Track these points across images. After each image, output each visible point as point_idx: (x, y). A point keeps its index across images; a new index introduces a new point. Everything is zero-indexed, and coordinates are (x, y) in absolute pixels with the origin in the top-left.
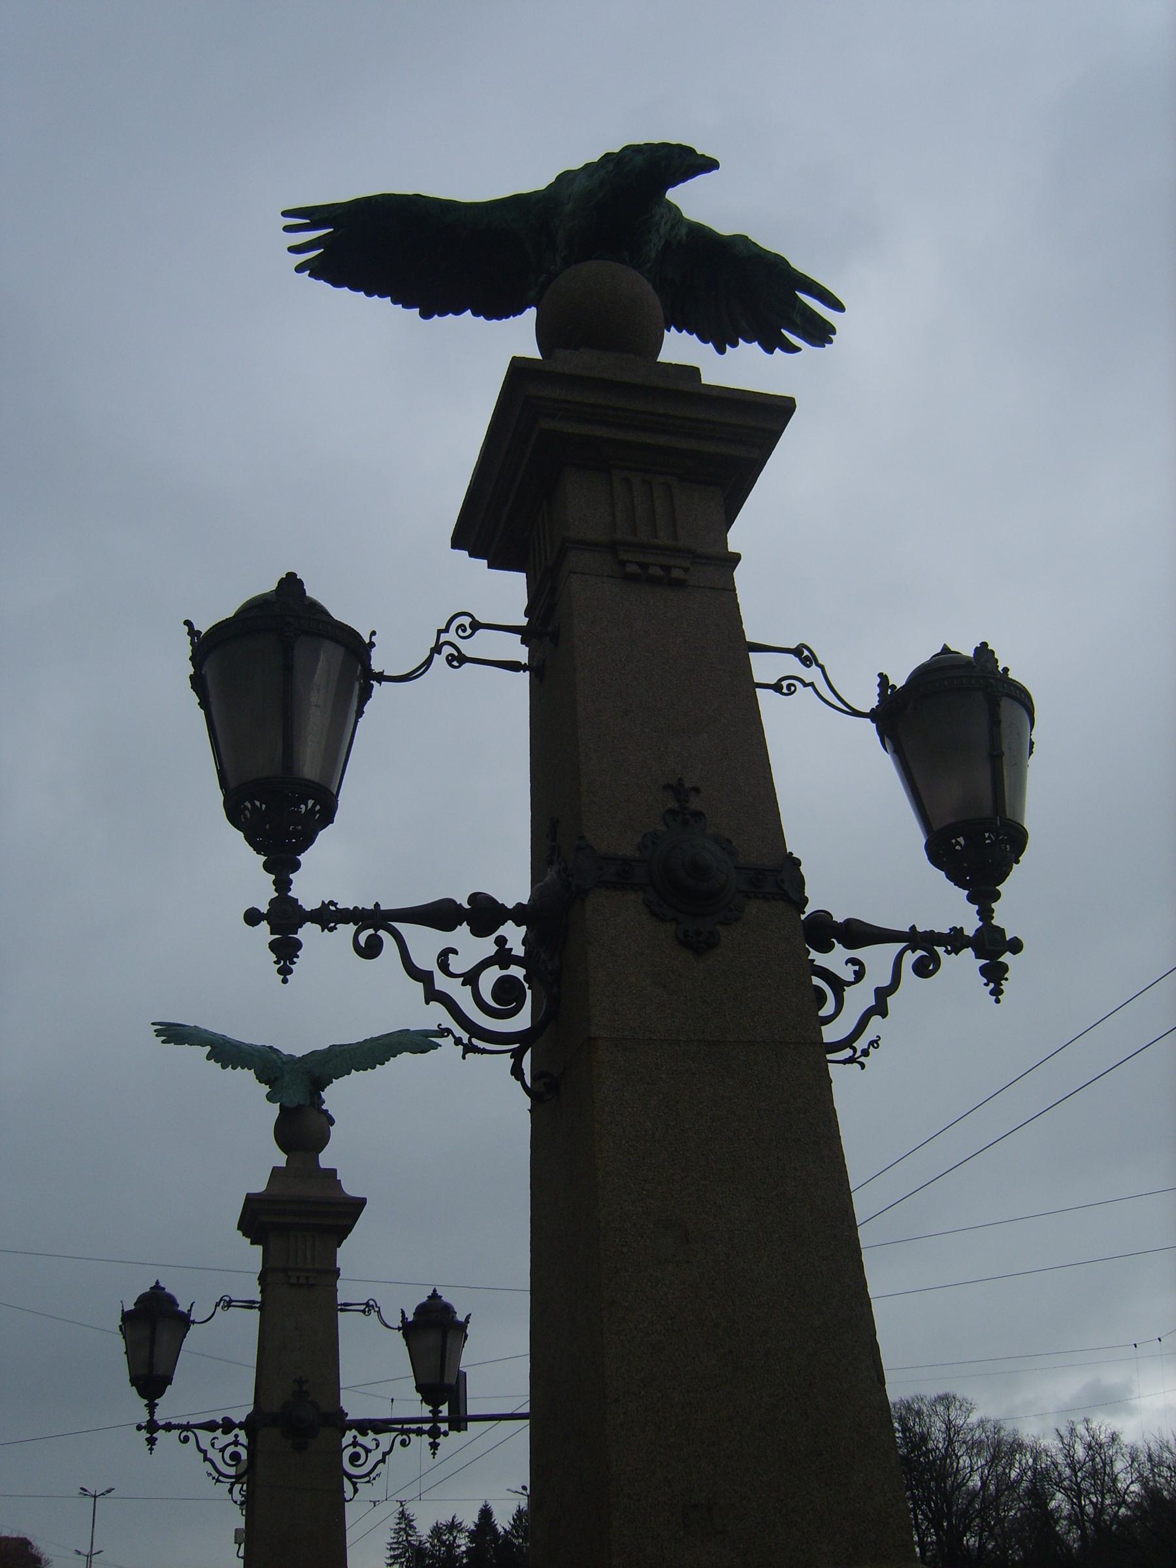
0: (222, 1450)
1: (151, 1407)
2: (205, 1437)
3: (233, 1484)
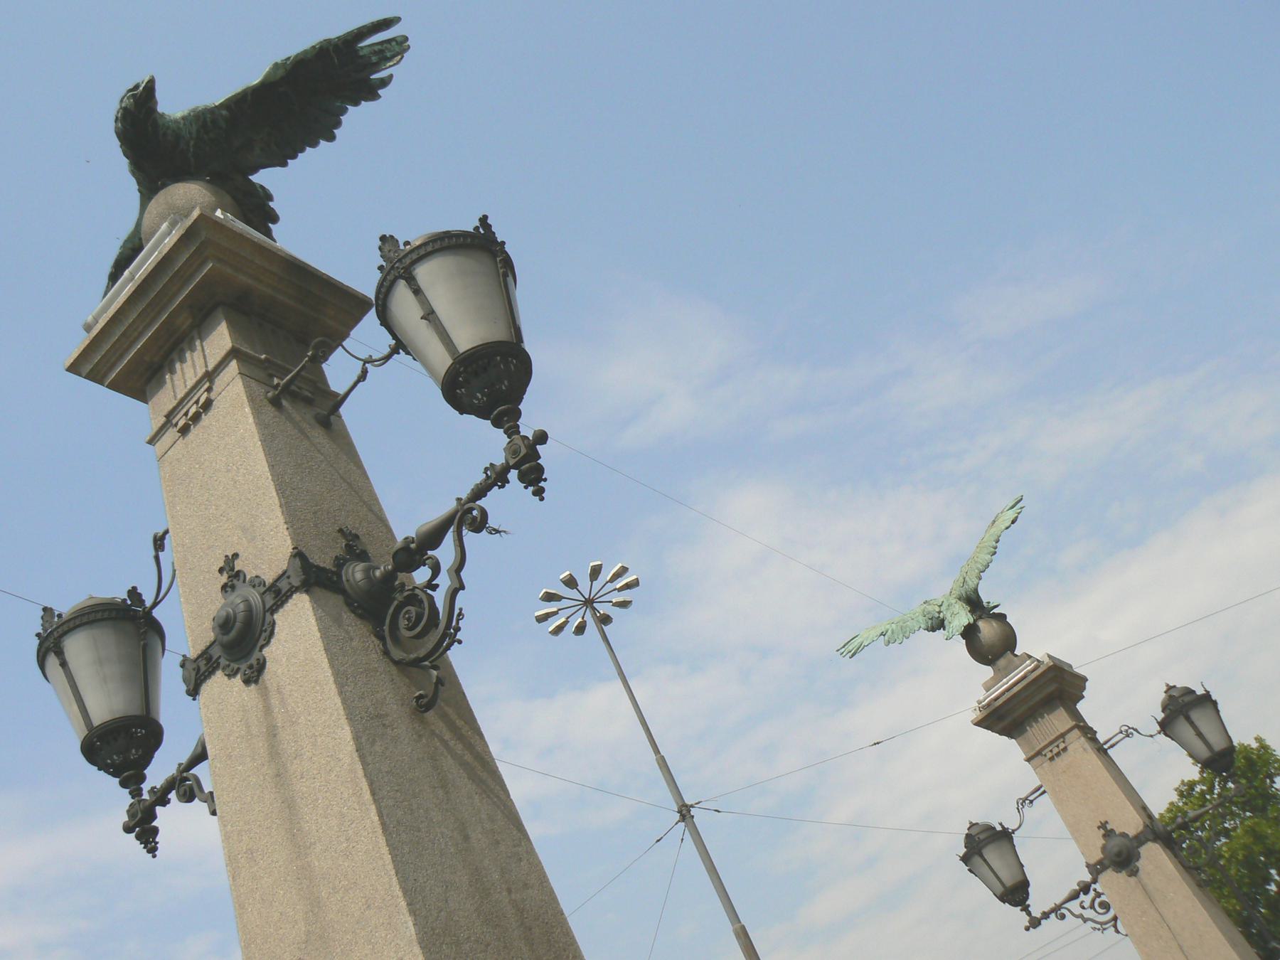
0: (1092, 907)
1: (1026, 909)
2: (1074, 906)
3: (1115, 926)
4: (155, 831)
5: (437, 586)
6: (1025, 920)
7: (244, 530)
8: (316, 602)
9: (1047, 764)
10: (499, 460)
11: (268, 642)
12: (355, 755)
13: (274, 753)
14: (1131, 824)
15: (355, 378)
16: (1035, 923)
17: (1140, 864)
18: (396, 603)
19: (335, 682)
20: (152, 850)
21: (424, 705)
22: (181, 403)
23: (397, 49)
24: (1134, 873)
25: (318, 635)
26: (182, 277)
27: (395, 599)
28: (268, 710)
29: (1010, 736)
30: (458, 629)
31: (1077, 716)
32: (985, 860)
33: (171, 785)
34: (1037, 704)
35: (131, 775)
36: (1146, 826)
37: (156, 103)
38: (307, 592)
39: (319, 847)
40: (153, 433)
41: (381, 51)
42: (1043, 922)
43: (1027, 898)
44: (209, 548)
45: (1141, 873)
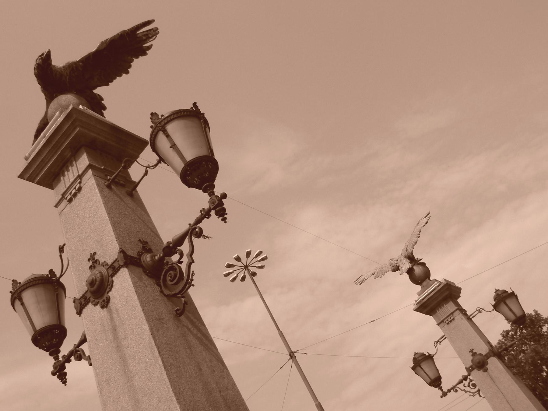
0: (469, 386)
1: (440, 388)
2: (461, 386)
3: (479, 394)
4: (65, 374)
5: (182, 262)
6: (440, 393)
7: (98, 242)
8: (131, 272)
9: (446, 326)
10: (207, 206)
11: (110, 290)
12: (151, 336)
13: (116, 337)
14: (483, 349)
15: (142, 175)
16: (445, 394)
17: (488, 366)
18: (165, 270)
19: (141, 305)
20: (65, 382)
21: (179, 313)
22: (68, 189)
23: (154, 33)
24: (486, 370)
25: (132, 285)
26: (66, 135)
27: (164, 268)
28: (112, 319)
29: (430, 315)
30: (192, 280)
31: (458, 305)
32: (422, 369)
33: (71, 354)
34: (441, 300)
35: (54, 351)
36: (490, 350)
37: (51, 61)
38: (127, 267)
39: (137, 377)
40: (57, 202)
41: (147, 35)
42: (448, 394)
43: (441, 384)
44: (83, 250)
45: (489, 370)
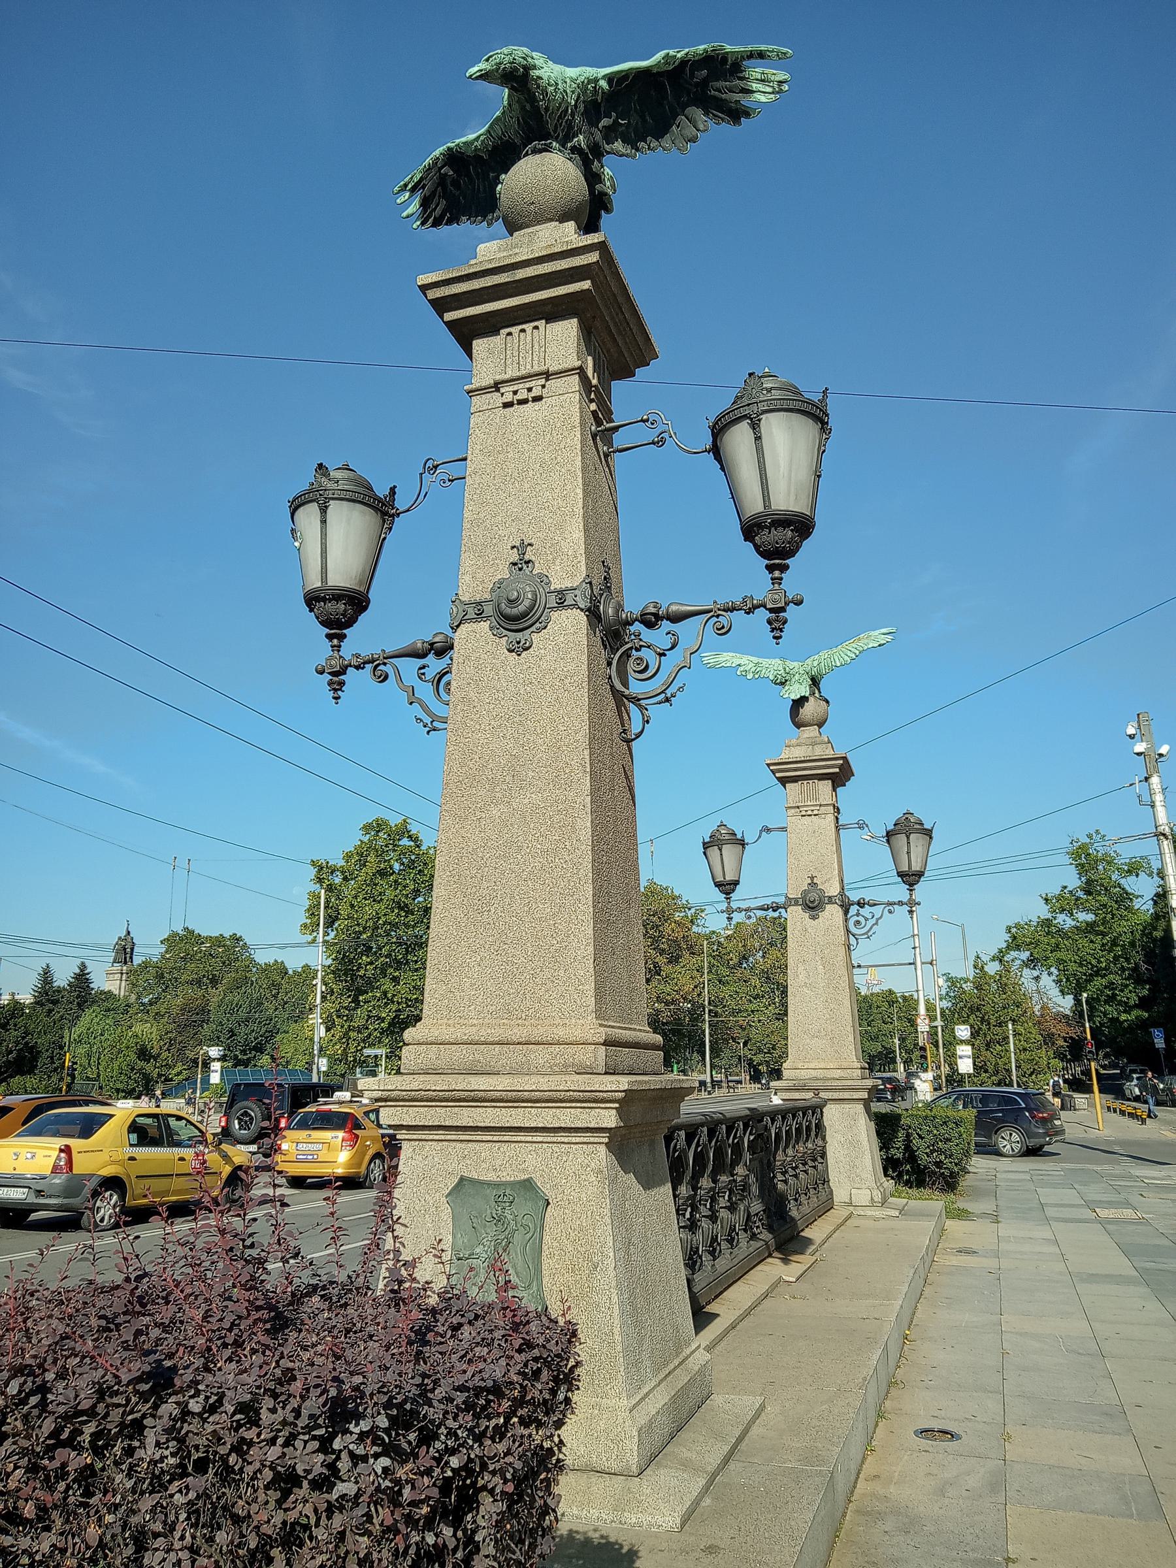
6: (724, 906)
10: (758, 598)
11: (539, 631)
14: (833, 890)
35: (337, 627)
